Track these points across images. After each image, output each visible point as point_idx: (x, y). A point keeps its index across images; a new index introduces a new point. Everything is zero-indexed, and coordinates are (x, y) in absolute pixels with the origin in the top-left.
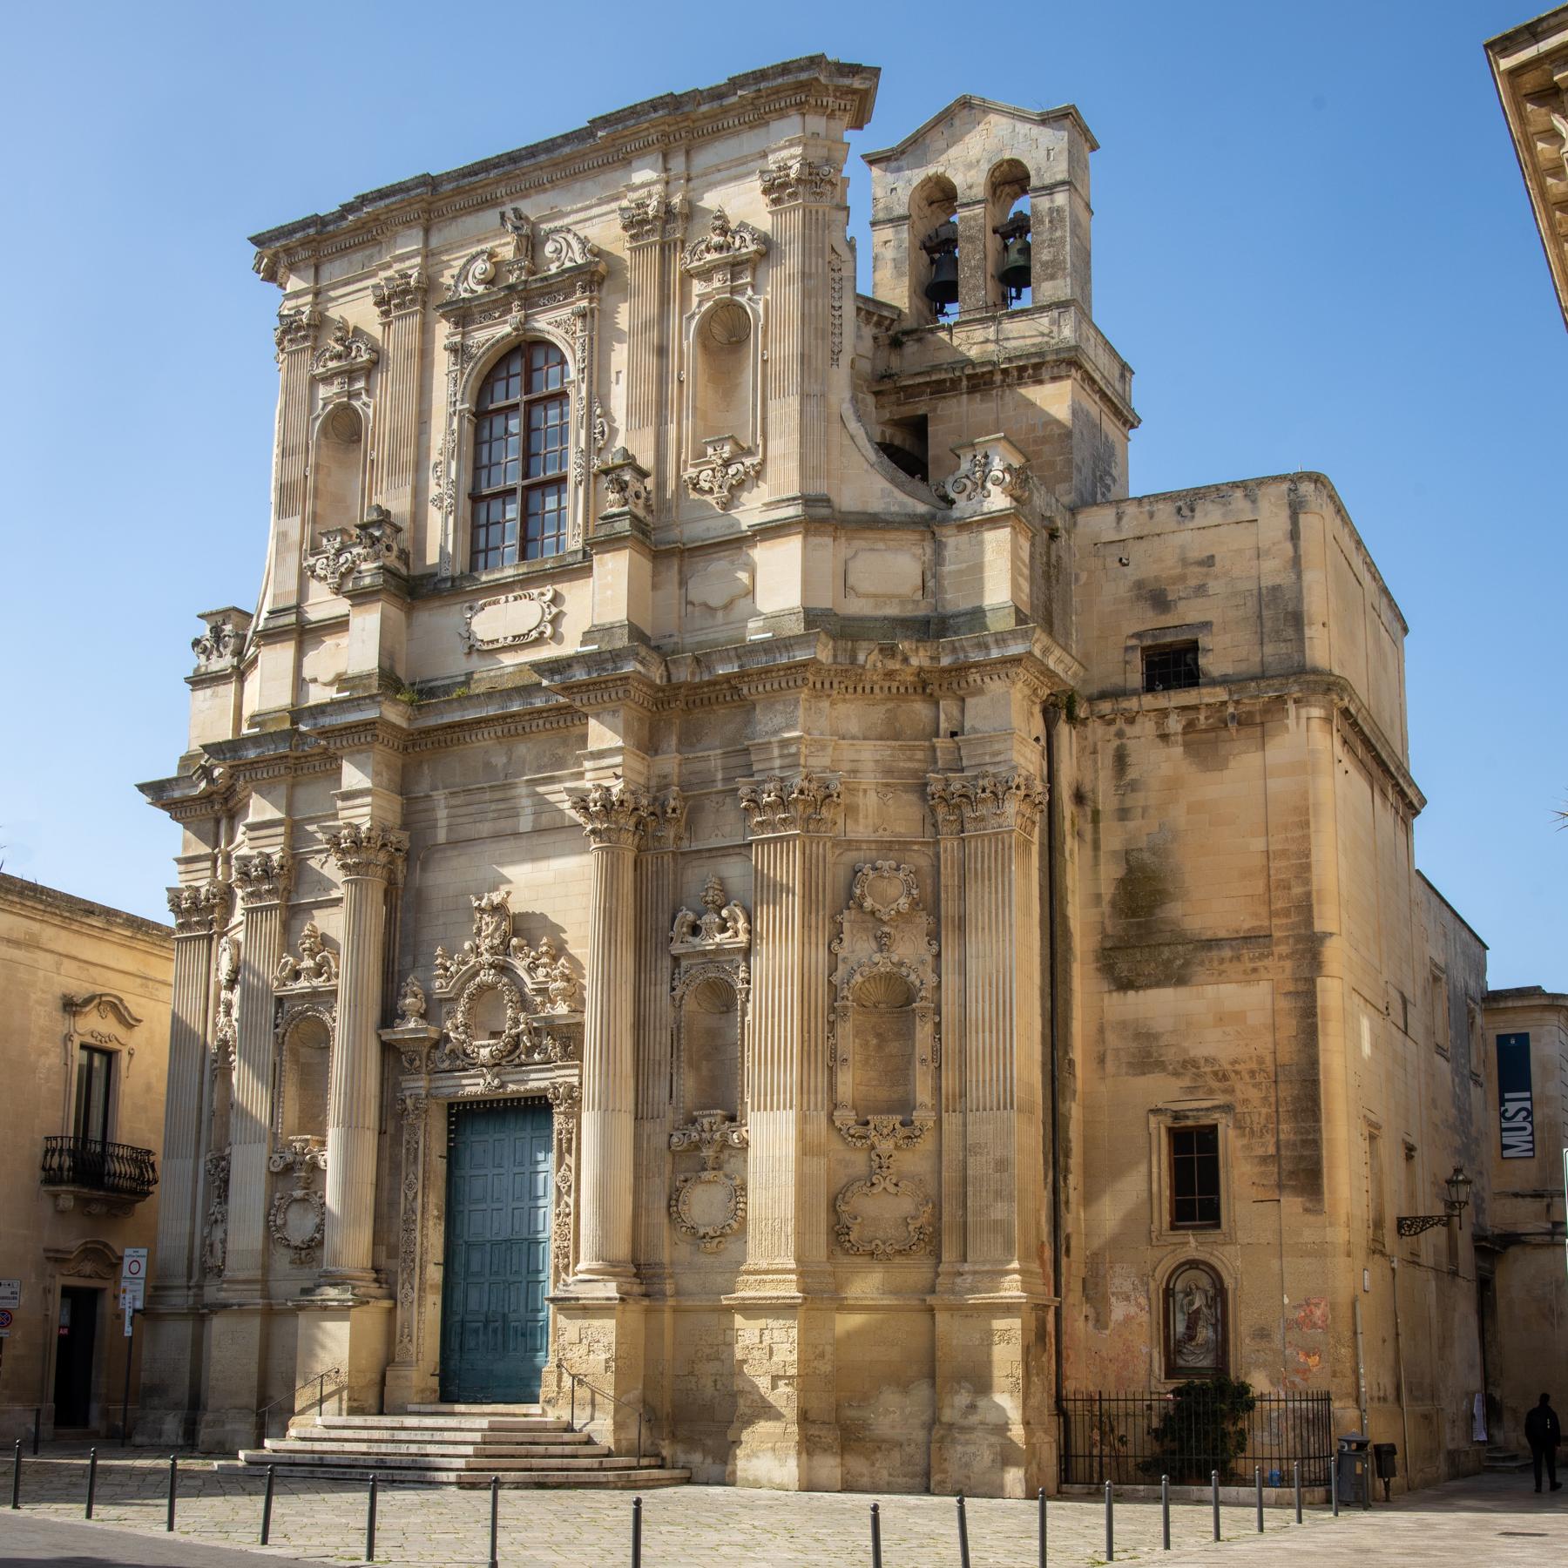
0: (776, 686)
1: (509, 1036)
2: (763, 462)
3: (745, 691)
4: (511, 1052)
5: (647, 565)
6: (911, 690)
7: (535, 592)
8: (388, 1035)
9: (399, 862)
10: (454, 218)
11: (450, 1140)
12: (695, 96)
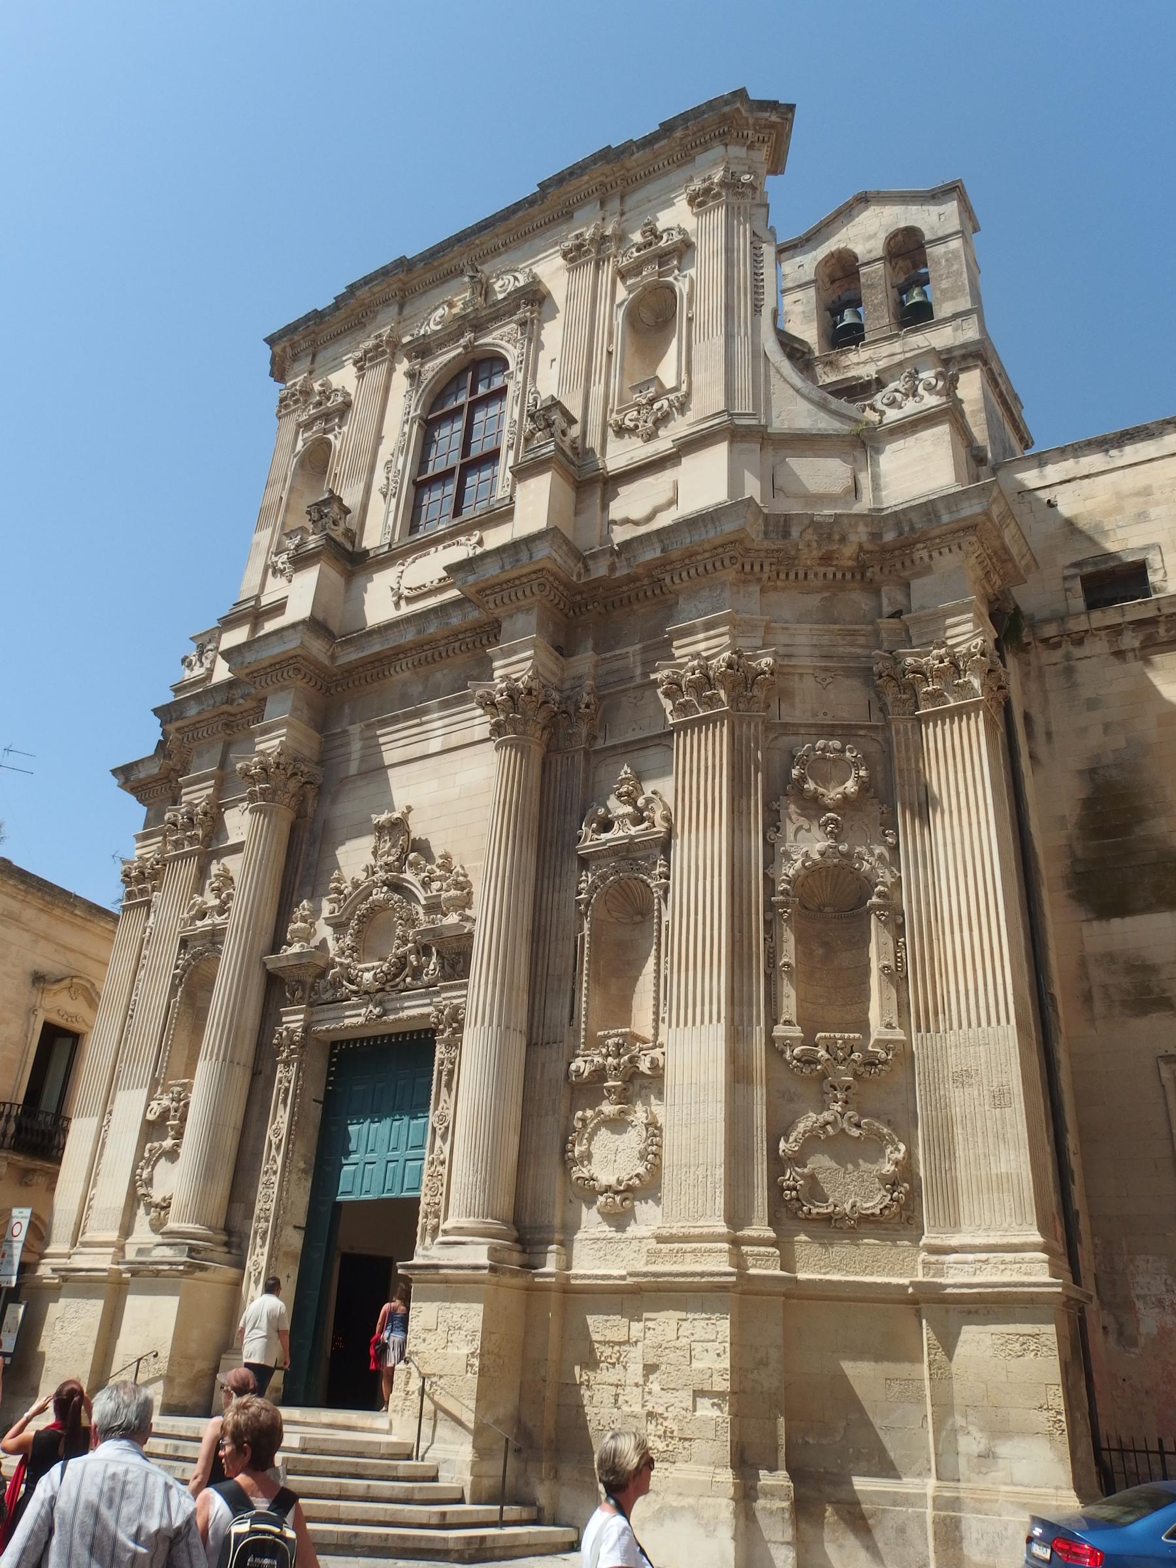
0: (701, 569)
1: (395, 956)
2: (688, 395)
3: (668, 580)
4: (396, 976)
5: (569, 494)
6: (848, 576)
7: (463, 539)
8: (273, 962)
9: (311, 795)
10: (425, 292)
11: (328, 1083)
12: (629, 148)
